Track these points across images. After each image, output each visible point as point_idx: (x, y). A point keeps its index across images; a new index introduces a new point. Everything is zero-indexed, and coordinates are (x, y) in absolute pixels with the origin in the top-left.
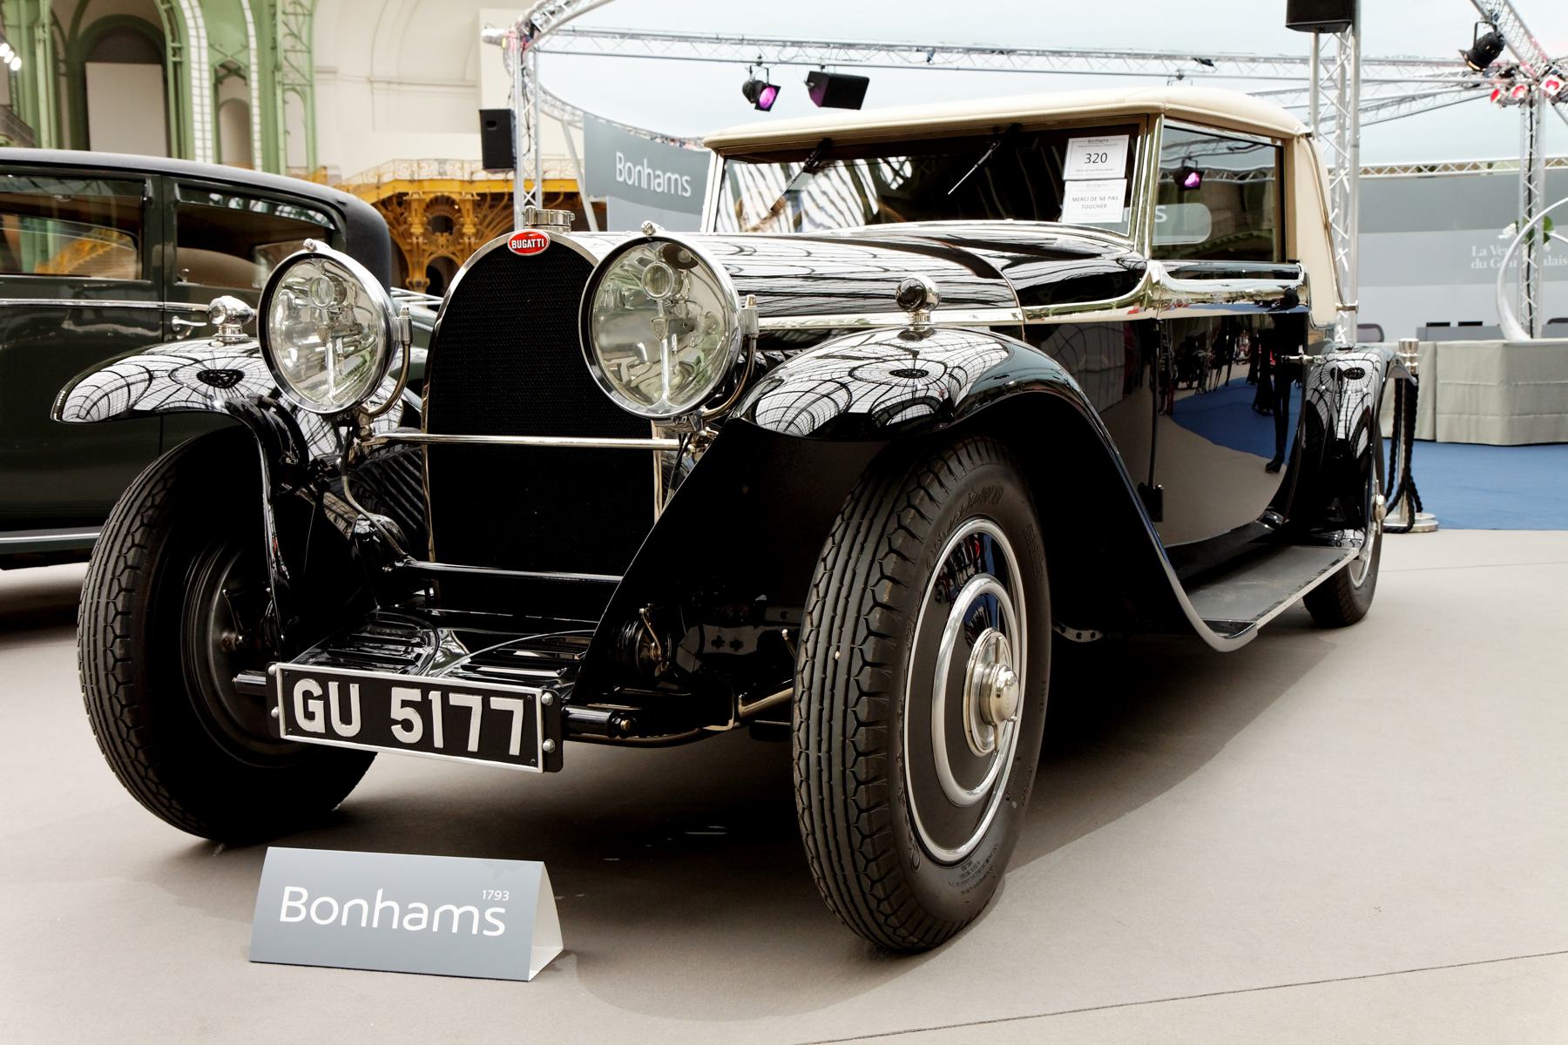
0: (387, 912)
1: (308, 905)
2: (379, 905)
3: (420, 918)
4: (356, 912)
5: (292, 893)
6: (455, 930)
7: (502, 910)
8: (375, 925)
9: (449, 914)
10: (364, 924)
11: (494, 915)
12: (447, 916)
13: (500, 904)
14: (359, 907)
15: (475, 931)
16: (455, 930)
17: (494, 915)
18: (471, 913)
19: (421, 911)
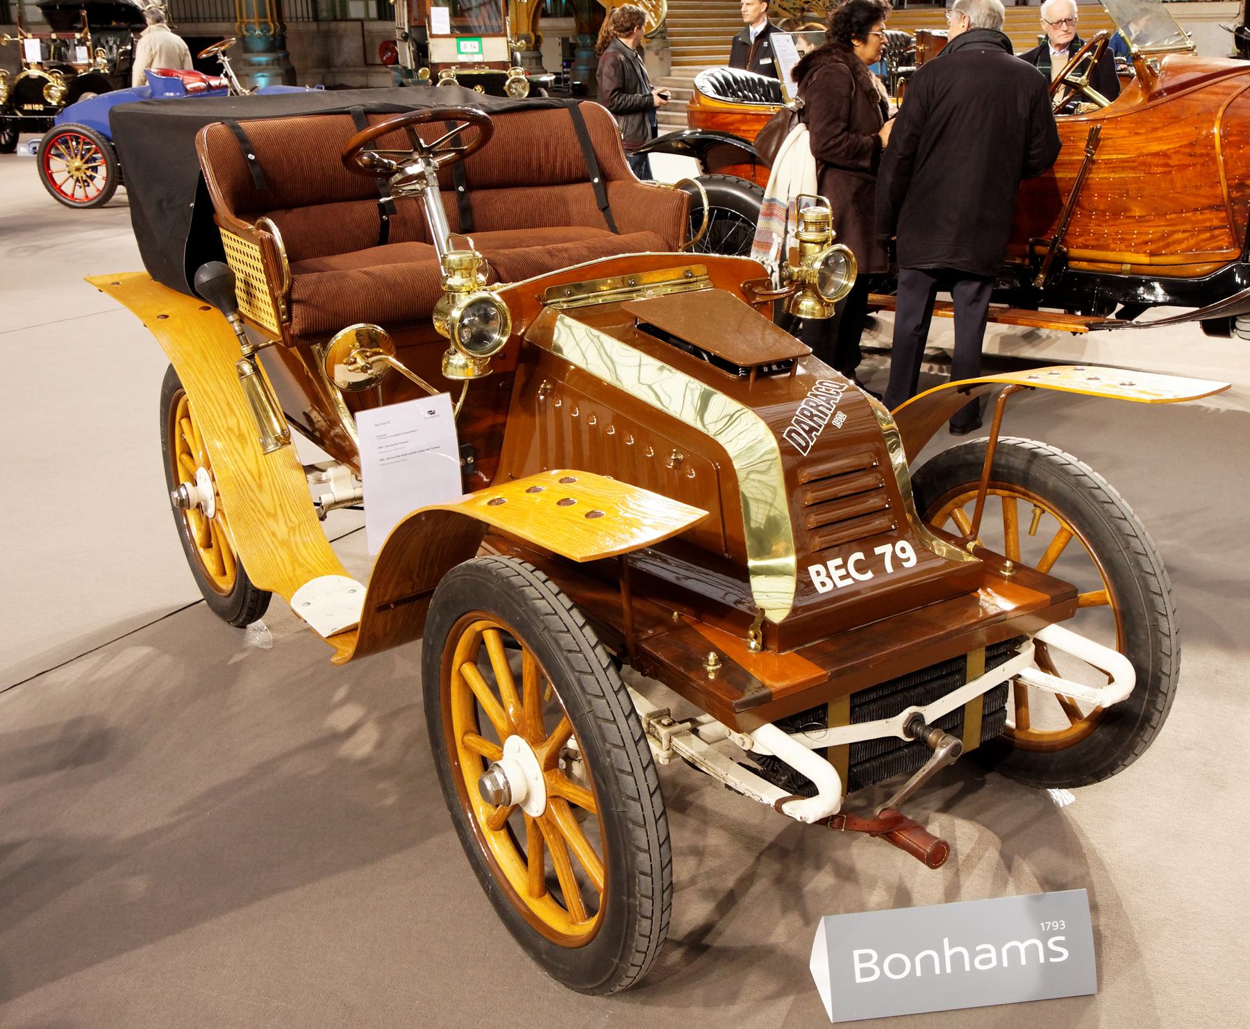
0: (957, 958)
1: (880, 963)
2: (948, 953)
4: (927, 962)
5: (860, 956)
6: (1023, 962)
7: (1063, 938)
8: (949, 970)
10: (938, 971)
11: (1056, 943)
12: (1014, 952)
13: (1058, 933)
14: (930, 958)
16: (1023, 962)
17: (1056, 943)
18: (1035, 946)
19: (988, 951)
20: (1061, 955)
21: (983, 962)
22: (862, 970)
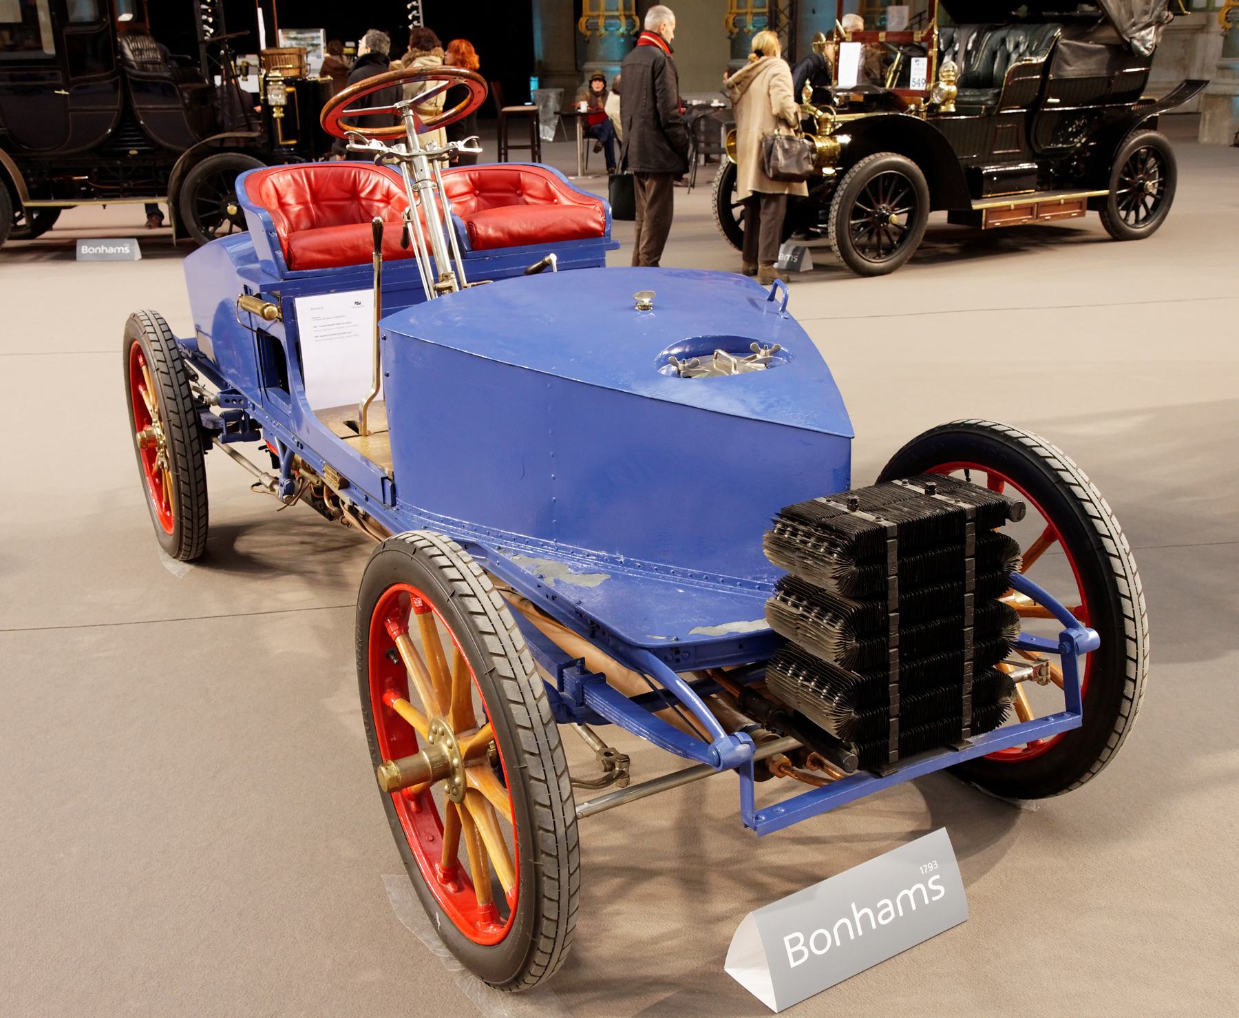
0: (865, 919)
1: (807, 944)
2: (857, 916)
3: (889, 911)
4: (844, 926)
6: (914, 908)
7: (938, 877)
8: (860, 933)
9: (906, 896)
10: (852, 937)
11: (935, 883)
12: (905, 899)
14: (844, 925)
15: (927, 902)
16: (914, 908)
17: (935, 883)
19: (886, 906)
21: (885, 917)
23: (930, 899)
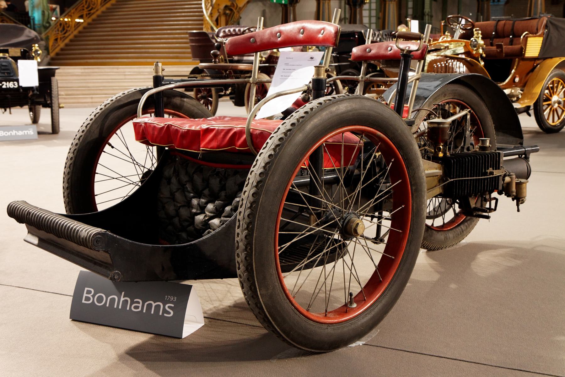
1: (93, 296)
4: (113, 300)
6: (152, 312)
7: (173, 305)
8: (120, 307)
9: (151, 305)
10: (115, 307)
11: (169, 307)
12: (150, 306)
14: (114, 299)
15: (161, 314)
16: (152, 312)
17: (169, 307)
18: (159, 306)
19: (139, 303)
20: (169, 313)
21: (136, 307)
22: (86, 297)
23: (163, 313)
